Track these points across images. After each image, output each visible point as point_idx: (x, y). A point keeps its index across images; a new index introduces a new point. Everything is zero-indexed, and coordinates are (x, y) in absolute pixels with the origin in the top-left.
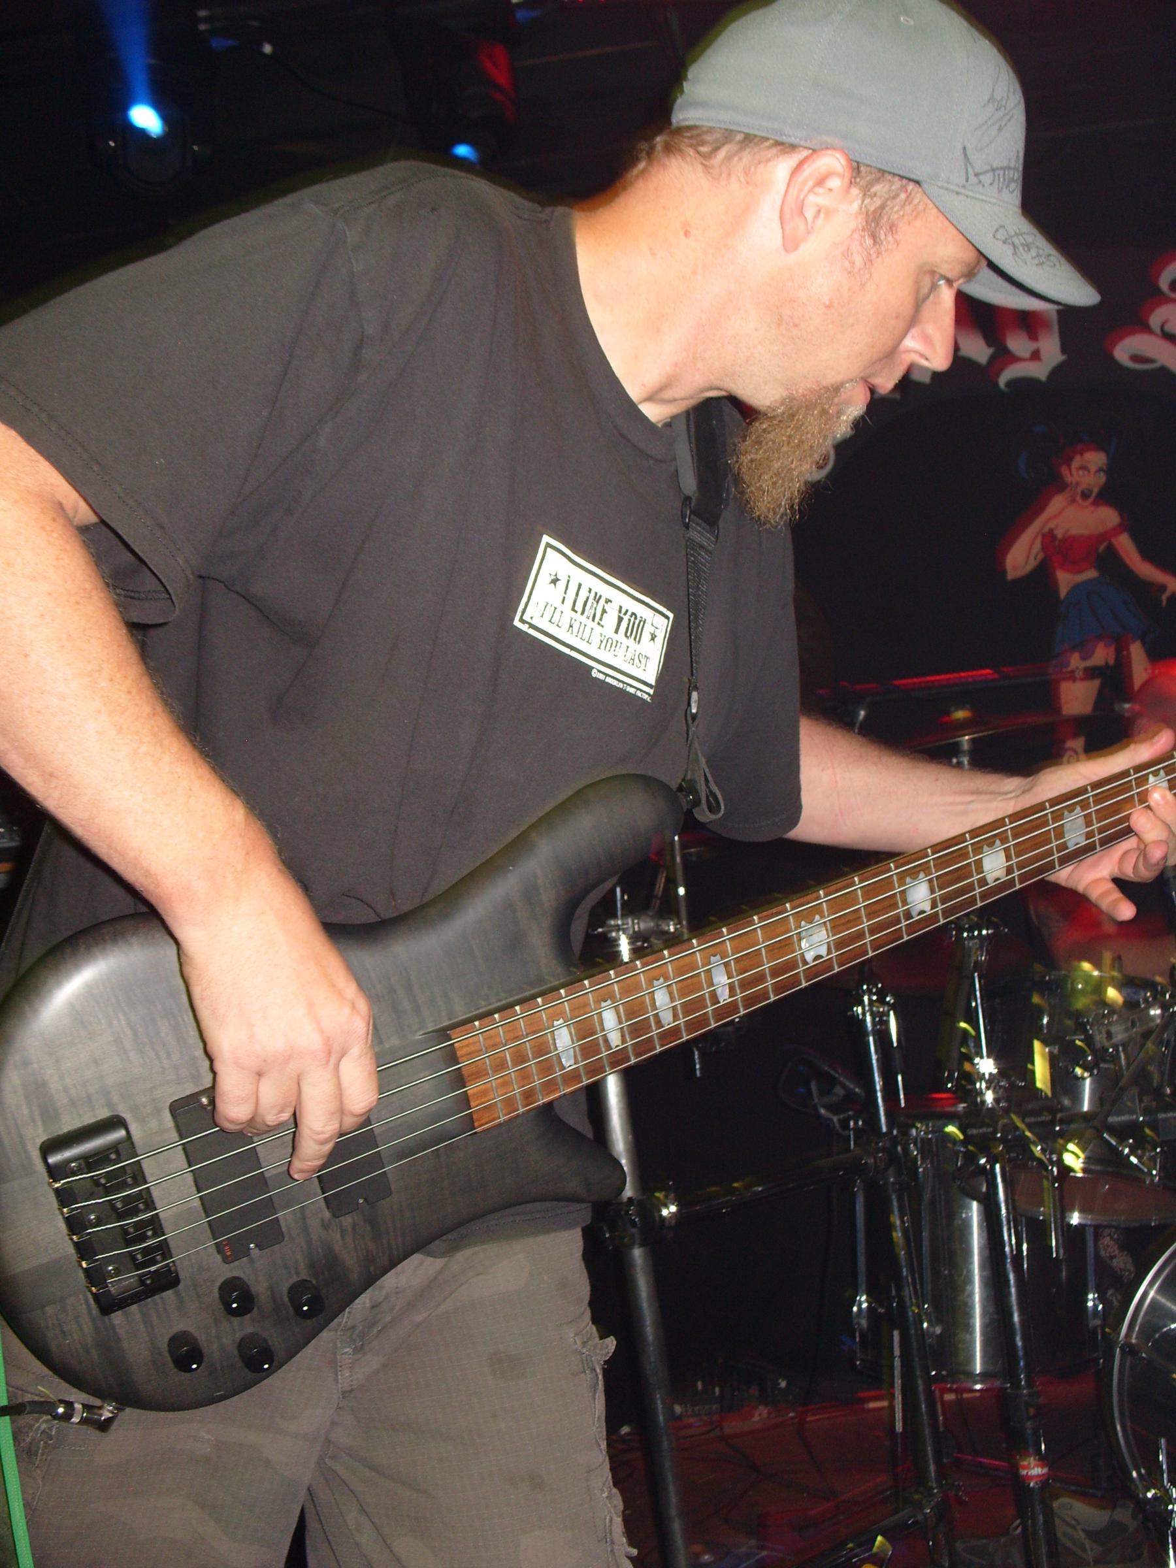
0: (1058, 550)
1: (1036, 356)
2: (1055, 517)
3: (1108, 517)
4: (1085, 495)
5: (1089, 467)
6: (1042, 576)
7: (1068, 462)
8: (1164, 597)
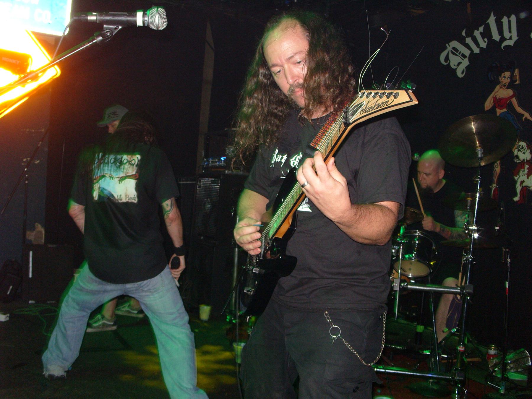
0: (499, 103)
1: (511, 38)
2: (497, 92)
3: (510, 92)
4: (504, 86)
6: (493, 110)
7: (501, 76)
8: (523, 118)
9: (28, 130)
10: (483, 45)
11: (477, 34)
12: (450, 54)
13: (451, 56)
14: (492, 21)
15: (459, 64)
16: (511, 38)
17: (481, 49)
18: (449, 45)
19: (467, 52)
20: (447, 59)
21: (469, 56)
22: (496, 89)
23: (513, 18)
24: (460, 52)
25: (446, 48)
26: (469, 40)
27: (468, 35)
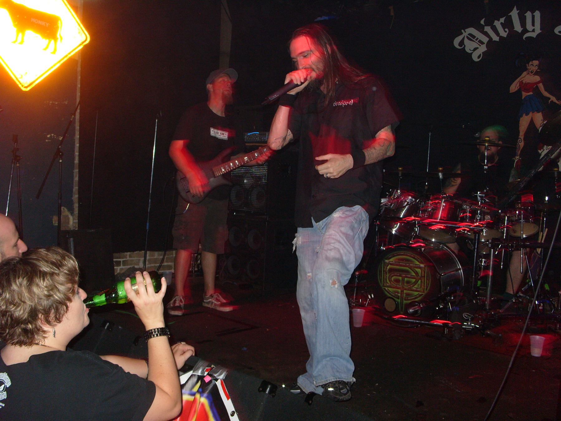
0: (524, 87)
3: (537, 78)
4: (532, 72)
5: (534, 65)
9: (51, 102)
10: (504, 34)
11: (497, 24)
12: (466, 41)
13: (466, 41)
14: (514, 14)
15: (475, 49)
16: (533, 31)
17: (501, 38)
18: (465, 32)
19: (485, 39)
20: (462, 43)
21: (487, 43)
22: (523, 75)
23: (537, 14)
24: (477, 39)
25: (462, 34)
26: (488, 29)
27: (487, 24)
